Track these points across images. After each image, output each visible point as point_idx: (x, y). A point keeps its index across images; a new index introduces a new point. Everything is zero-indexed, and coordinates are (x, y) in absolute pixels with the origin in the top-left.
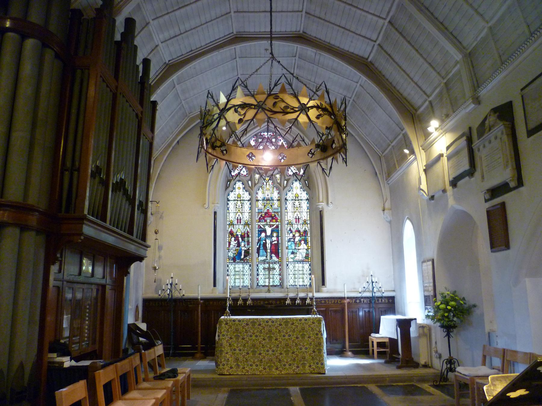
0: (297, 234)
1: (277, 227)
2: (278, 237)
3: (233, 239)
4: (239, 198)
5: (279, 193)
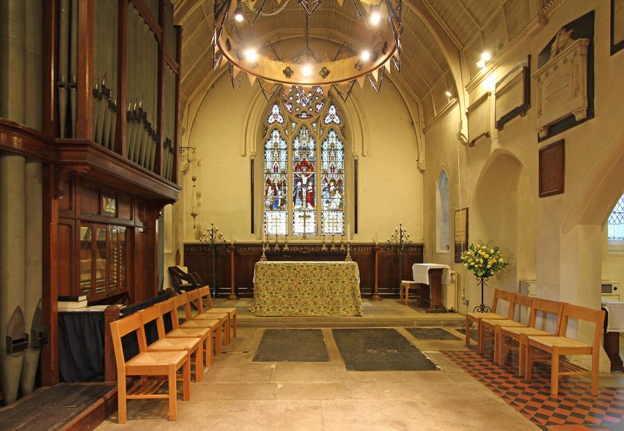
0: (332, 184)
1: (313, 176)
2: (313, 186)
3: (270, 187)
4: (276, 148)
5: (315, 143)
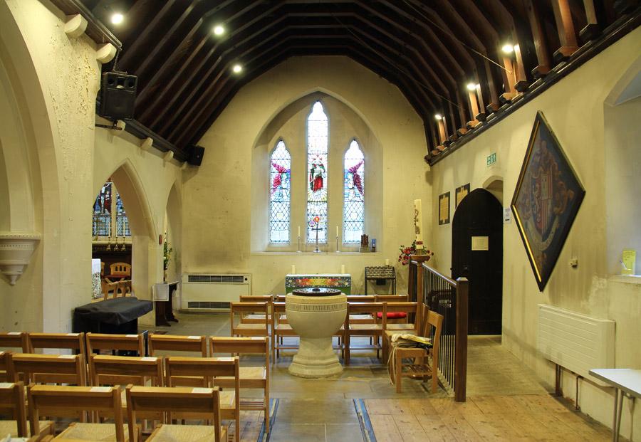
2: (110, 194)
